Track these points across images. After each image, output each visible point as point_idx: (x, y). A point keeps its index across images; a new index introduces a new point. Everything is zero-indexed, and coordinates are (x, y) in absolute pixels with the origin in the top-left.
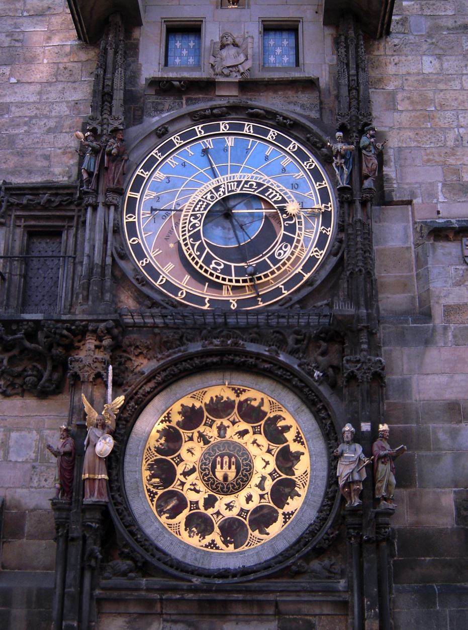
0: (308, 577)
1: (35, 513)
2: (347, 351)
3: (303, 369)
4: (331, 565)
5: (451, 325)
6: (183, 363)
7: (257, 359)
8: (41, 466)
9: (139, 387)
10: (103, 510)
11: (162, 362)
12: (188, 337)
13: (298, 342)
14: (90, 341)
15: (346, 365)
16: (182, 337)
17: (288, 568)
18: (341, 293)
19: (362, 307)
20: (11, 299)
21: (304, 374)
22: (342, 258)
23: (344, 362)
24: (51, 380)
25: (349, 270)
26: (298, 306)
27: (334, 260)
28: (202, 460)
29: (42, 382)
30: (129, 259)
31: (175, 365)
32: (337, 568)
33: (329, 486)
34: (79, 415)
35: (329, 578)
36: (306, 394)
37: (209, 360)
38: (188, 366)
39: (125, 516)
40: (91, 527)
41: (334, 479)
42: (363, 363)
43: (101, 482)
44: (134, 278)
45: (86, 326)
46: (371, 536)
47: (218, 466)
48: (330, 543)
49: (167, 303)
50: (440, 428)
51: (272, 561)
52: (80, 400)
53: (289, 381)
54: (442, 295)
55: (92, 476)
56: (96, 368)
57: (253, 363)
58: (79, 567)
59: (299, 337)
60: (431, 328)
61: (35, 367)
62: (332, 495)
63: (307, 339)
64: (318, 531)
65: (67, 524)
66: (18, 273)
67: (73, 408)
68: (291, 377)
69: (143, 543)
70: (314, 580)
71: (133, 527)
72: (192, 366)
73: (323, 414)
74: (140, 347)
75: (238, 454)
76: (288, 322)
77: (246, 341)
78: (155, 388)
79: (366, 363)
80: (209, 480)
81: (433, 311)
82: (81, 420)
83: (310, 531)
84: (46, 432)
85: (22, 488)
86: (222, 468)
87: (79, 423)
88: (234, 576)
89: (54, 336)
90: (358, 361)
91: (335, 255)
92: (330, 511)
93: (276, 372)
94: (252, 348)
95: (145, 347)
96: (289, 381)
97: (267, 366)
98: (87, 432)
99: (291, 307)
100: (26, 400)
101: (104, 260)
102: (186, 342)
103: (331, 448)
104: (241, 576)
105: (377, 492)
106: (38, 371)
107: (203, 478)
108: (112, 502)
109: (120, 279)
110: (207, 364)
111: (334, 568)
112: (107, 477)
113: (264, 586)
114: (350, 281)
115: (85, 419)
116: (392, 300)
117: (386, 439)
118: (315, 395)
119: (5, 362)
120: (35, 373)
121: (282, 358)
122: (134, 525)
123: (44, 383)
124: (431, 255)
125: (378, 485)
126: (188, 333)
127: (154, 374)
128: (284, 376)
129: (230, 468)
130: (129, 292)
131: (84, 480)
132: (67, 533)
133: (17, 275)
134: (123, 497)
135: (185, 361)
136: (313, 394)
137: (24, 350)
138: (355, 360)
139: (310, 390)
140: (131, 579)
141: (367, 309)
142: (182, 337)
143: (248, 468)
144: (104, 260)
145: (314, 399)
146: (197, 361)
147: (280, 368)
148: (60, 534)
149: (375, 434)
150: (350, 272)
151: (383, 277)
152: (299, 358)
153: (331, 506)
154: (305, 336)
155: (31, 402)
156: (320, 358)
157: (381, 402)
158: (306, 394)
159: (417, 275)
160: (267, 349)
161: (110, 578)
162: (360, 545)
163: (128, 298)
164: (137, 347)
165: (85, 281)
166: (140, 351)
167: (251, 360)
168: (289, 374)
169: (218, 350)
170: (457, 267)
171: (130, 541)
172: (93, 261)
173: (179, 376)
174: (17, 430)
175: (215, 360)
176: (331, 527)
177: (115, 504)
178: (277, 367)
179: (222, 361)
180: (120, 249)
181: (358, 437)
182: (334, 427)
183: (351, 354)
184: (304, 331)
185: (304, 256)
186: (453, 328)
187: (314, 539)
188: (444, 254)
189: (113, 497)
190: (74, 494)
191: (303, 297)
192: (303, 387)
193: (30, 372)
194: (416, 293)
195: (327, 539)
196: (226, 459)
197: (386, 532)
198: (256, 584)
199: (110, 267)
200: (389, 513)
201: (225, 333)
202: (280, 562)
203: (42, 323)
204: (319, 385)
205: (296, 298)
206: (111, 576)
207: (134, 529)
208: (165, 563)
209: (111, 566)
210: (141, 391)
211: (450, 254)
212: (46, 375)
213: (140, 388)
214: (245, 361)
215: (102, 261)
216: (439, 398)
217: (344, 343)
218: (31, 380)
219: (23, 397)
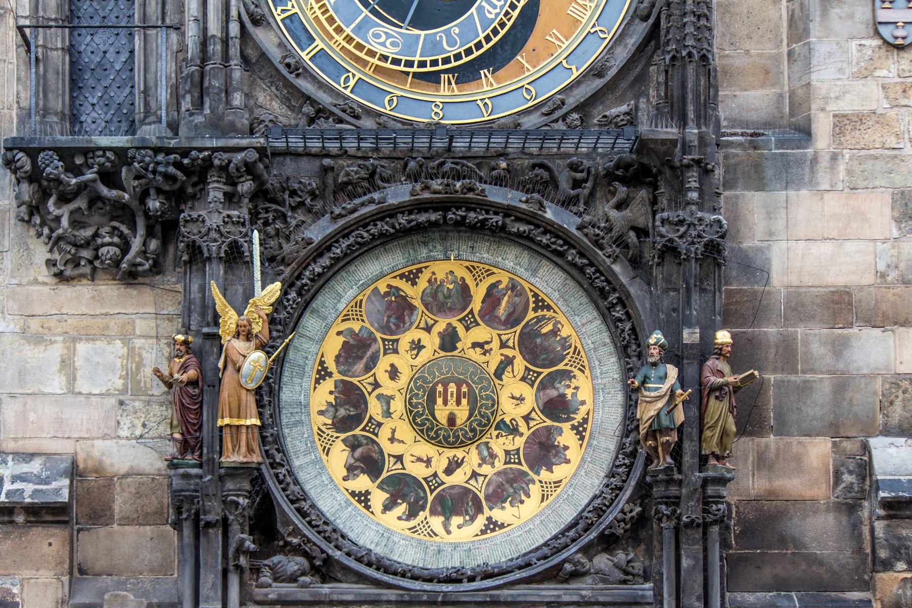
0: (590, 581)
1: (129, 480)
2: (664, 202)
3: (586, 235)
4: (629, 562)
5: (845, 151)
6: (378, 223)
7: (506, 215)
8: (134, 400)
9: (304, 265)
10: (252, 475)
11: (341, 222)
12: (384, 174)
13: (576, 184)
14: (215, 185)
15: (661, 229)
16: (372, 174)
17: (559, 567)
18: (652, 92)
19: (691, 123)
20: (50, 96)
21: (589, 244)
22: (657, 25)
23: (658, 223)
24: (145, 252)
25: (669, 52)
26: (575, 116)
27: (641, 29)
28: (412, 390)
29: (129, 257)
30: (269, 23)
31: (365, 226)
32: (638, 566)
33: (626, 433)
34: (203, 315)
35: (625, 582)
36: (590, 278)
37: (422, 218)
38: (386, 227)
39: (288, 484)
40: (237, 504)
41: (635, 423)
42: (689, 225)
43: (250, 430)
44: (281, 63)
45: (208, 163)
46: (693, 517)
47: (440, 401)
48: (628, 527)
49: (344, 111)
50: (815, 335)
51: (533, 555)
52: (203, 289)
53: (561, 255)
54: (832, 95)
55: (236, 422)
56: (229, 233)
57: (500, 223)
58: (220, 568)
59: (579, 176)
60: (810, 157)
61: (114, 228)
62: (631, 449)
63: (591, 178)
64: (608, 507)
65: (196, 500)
66: (59, 46)
67: (190, 304)
68: (565, 247)
69: (321, 529)
70: (601, 586)
71: (299, 499)
72: (394, 227)
73: (618, 312)
74: (299, 192)
75: (472, 380)
76: (559, 148)
77: (485, 183)
78: (332, 265)
79: (695, 225)
80: (423, 424)
81: (813, 126)
82: (208, 325)
83: (595, 509)
84: (138, 343)
85: (104, 437)
86: (445, 403)
87: (205, 330)
88: (472, 579)
89: (152, 176)
90: (681, 222)
91: (645, 19)
92: (628, 475)
93: (539, 239)
94: (498, 195)
95: (308, 192)
96: (561, 255)
97: (523, 228)
98: (221, 346)
99: (564, 118)
100: (99, 285)
101: (226, 29)
102: (380, 182)
103: (631, 369)
104: (482, 579)
105: (704, 445)
106: (121, 236)
107: (414, 420)
108: (267, 461)
109: (256, 63)
110: (418, 224)
111: (633, 567)
112: (259, 423)
113: (520, 595)
114: (670, 73)
115: (217, 324)
116: (745, 100)
117: (724, 356)
118: (607, 281)
119: (65, 222)
120: (116, 240)
121: (549, 215)
122: (305, 500)
123: (135, 257)
124: (818, 19)
125: (708, 433)
126: (382, 166)
127: (328, 244)
128: (554, 246)
129: (458, 403)
130: (273, 89)
131: (221, 427)
132: (197, 514)
133: (57, 49)
134: (283, 452)
135: (382, 219)
136: (603, 278)
137: (95, 200)
138: (676, 219)
139: (598, 271)
140: (305, 586)
141: (699, 127)
142: (372, 174)
143: (490, 402)
144: (226, 29)
145: (604, 288)
146: (402, 220)
147: (545, 232)
148: (184, 516)
149: (706, 350)
150: (671, 55)
151: (728, 56)
152: (579, 214)
153: (630, 467)
154: (589, 172)
155: (109, 289)
156: (614, 214)
157: (717, 293)
158: (590, 278)
159: (790, 54)
160: (524, 199)
161: (270, 586)
162: (677, 530)
163: (271, 100)
164: (293, 193)
165: (194, 68)
166: (299, 199)
167: (496, 218)
168: (560, 242)
169: (441, 201)
170: (863, 42)
171: (300, 526)
172: (205, 29)
173: (370, 246)
174: (87, 340)
175: (434, 216)
176: (628, 502)
177: (273, 465)
178: (542, 229)
179: (445, 217)
180: (253, 7)
181: (674, 354)
182: (636, 335)
183: (670, 208)
184: (586, 163)
185: (586, 18)
186: (847, 156)
187: (601, 520)
188: (840, 18)
189: (267, 454)
190: (205, 450)
191: (587, 100)
192: (587, 265)
193: (107, 239)
194: (786, 88)
195: (624, 520)
196: (452, 388)
197: (719, 510)
198: (506, 592)
199: (237, 41)
200: (722, 481)
201: (448, 165)
202: (545, 557)
203: (131, 153)
204: (612, 263)
205: (572, 101)
206: (270, 581)
207: (305, 506)
208: (359, 560)
209: (269, 566)
210: (307, 273)
211: (851, 16)
212: (136, 244)
213: (305, 268)
214: (486, 220)
215: (222, 27)
216: (817, 283)
217: (656, 188)
218: (111, 253)
219: (93, 280)
